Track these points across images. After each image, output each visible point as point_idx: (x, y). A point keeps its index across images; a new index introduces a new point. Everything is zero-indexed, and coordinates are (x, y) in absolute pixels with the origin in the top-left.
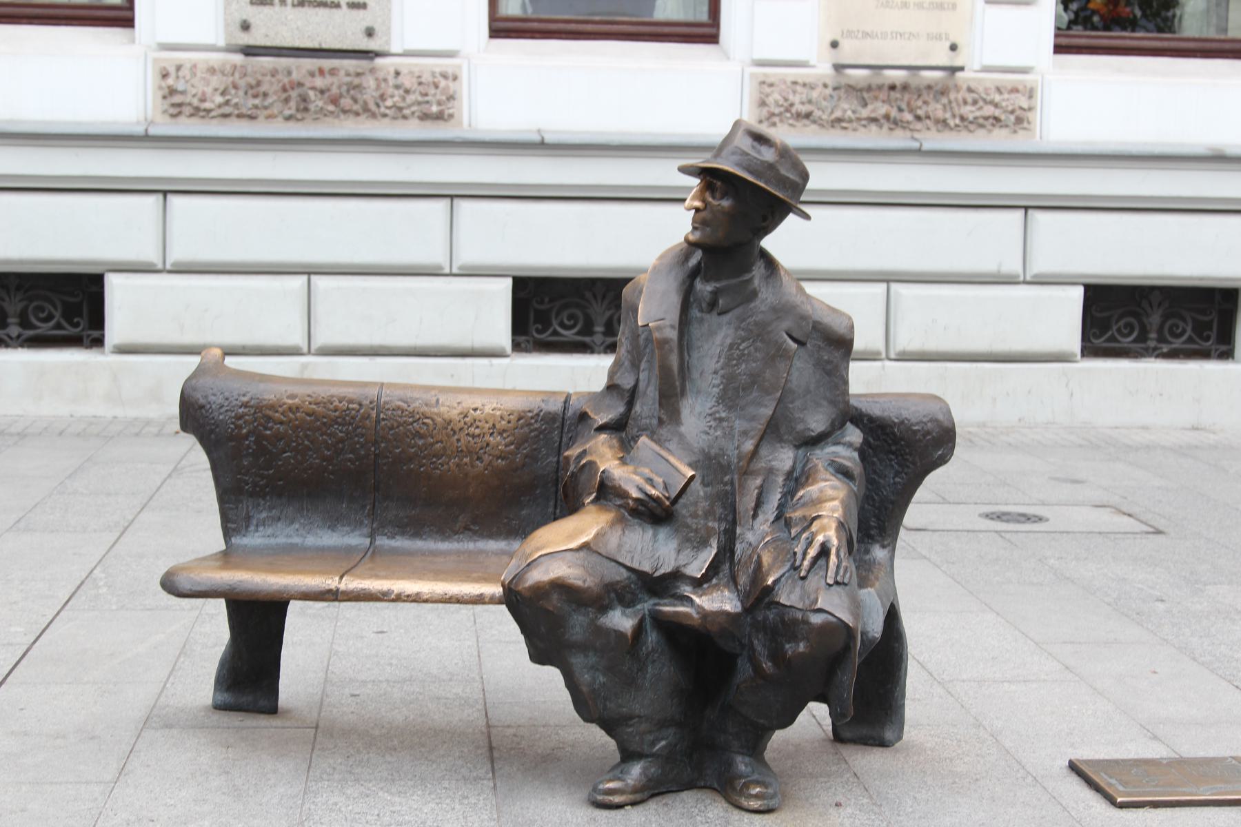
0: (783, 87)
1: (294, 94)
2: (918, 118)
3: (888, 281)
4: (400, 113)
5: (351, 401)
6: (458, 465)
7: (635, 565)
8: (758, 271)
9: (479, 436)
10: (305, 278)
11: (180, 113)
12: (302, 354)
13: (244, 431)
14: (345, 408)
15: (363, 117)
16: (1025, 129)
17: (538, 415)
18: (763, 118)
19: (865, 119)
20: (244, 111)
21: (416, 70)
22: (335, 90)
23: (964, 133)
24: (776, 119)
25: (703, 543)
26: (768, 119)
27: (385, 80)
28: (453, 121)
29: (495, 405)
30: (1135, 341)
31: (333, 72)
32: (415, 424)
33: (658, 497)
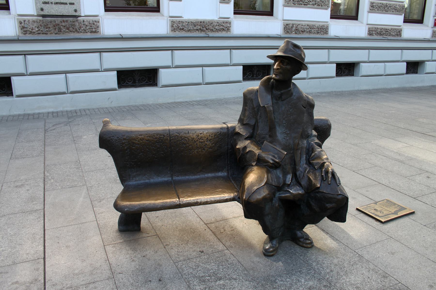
1: (57, 27)
2: (207, 29)
3: (202, 67)
4: (85, 31)
5: (161, 135)
6: (197, 152)
9: (203, 142)
10: (65, 74)
11: (26, 33)
13: (126, 148)
14: (159, 137)
15: (76, 33)
16: (229, 31)
17: (220, 134)
20: (44, 32)
21: (88, 20)
22: (68, 26)
23: (217, 32)
24: (176, 30)
26: (174, 30)
27: (81, 23)
28: (99, 33)
29: (206, 132)
30: (251, 77)
31: (67, 21)
32: (182, 140)
33: (279, 162)
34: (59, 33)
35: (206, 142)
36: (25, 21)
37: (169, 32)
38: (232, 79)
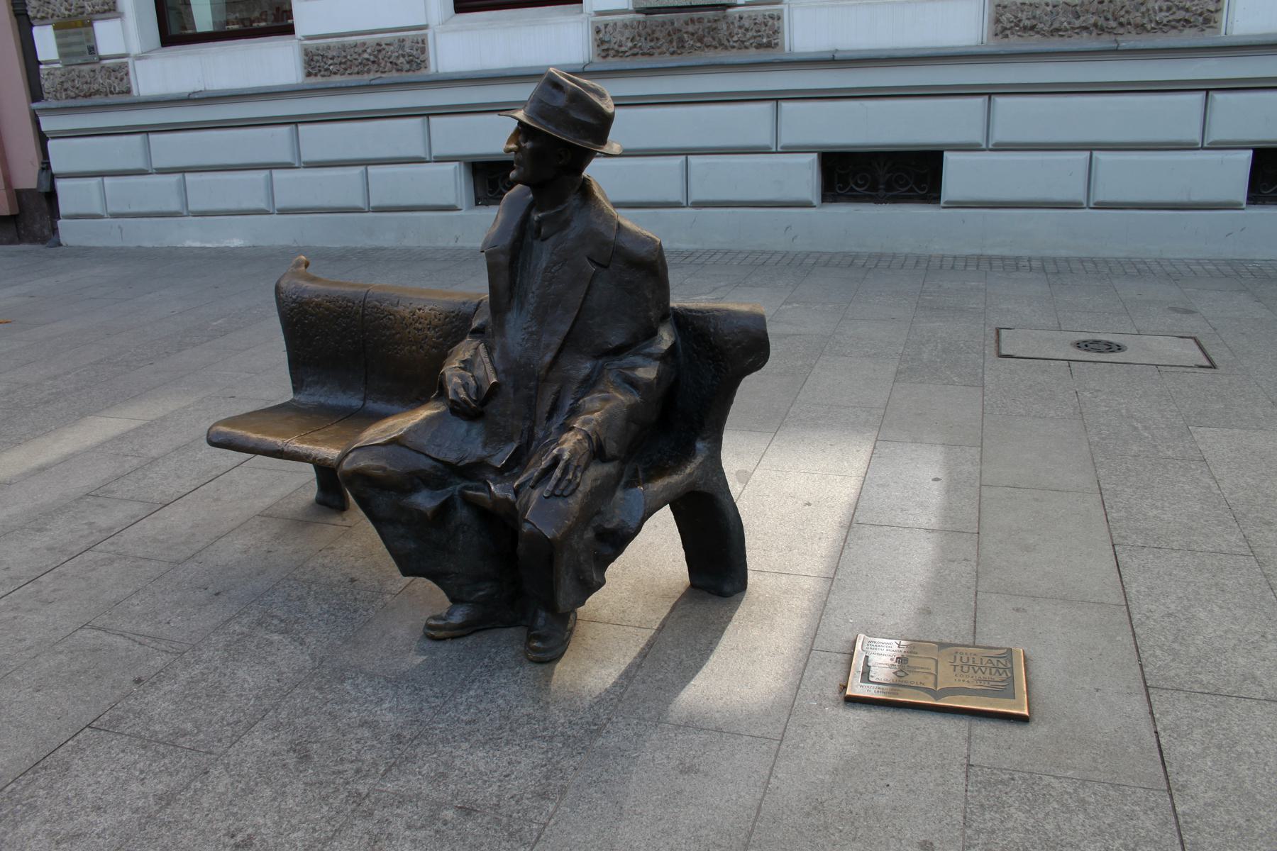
0: (1014, 8)
1: (675, 37)
2: (1121, 25)
3: (1091, 150)
4: (742, 45)
5: (349, 301)
7: (441, 457)
8: (573, 201)
11: (607, 55)
12: (684, 207)
15: (720, 49)
17: (458, 315)
18: (998, 32)
19: (1078, 28)
20: (645, 51)
21: (753, 14)
22: (700, 32)
23: (1159, 34)
24: (1008, 32)
25: (510, 439)
26: (1002, 32)
27: (733, 23)
31: (700, 20)
34: (679, 52)
36: (606, 26)
37: (985, 41)
38: (1196, 197)
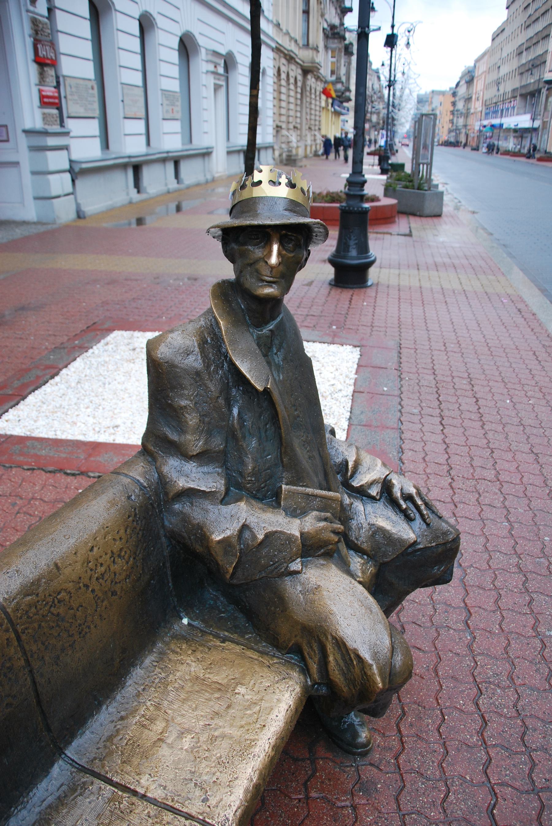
35: (112, 568)
